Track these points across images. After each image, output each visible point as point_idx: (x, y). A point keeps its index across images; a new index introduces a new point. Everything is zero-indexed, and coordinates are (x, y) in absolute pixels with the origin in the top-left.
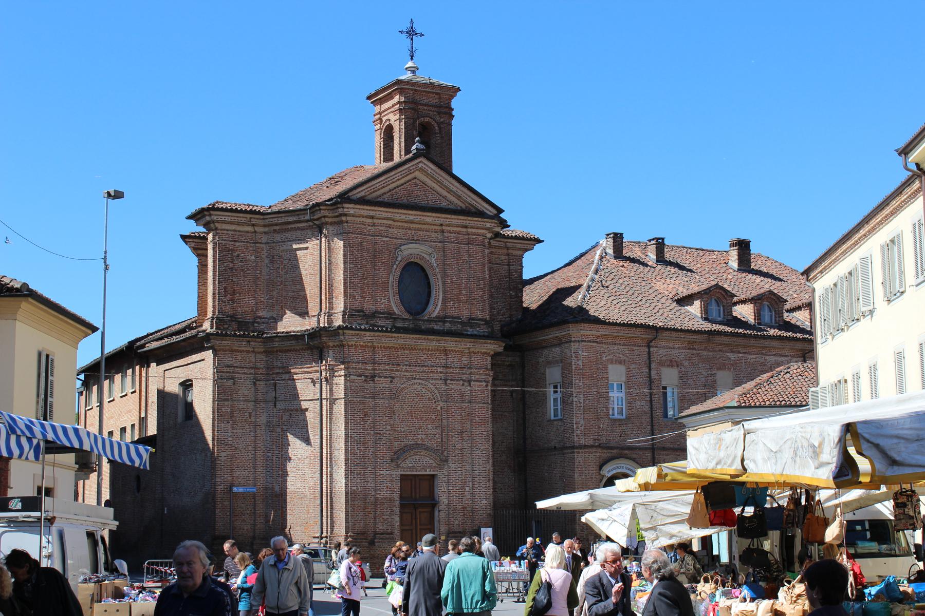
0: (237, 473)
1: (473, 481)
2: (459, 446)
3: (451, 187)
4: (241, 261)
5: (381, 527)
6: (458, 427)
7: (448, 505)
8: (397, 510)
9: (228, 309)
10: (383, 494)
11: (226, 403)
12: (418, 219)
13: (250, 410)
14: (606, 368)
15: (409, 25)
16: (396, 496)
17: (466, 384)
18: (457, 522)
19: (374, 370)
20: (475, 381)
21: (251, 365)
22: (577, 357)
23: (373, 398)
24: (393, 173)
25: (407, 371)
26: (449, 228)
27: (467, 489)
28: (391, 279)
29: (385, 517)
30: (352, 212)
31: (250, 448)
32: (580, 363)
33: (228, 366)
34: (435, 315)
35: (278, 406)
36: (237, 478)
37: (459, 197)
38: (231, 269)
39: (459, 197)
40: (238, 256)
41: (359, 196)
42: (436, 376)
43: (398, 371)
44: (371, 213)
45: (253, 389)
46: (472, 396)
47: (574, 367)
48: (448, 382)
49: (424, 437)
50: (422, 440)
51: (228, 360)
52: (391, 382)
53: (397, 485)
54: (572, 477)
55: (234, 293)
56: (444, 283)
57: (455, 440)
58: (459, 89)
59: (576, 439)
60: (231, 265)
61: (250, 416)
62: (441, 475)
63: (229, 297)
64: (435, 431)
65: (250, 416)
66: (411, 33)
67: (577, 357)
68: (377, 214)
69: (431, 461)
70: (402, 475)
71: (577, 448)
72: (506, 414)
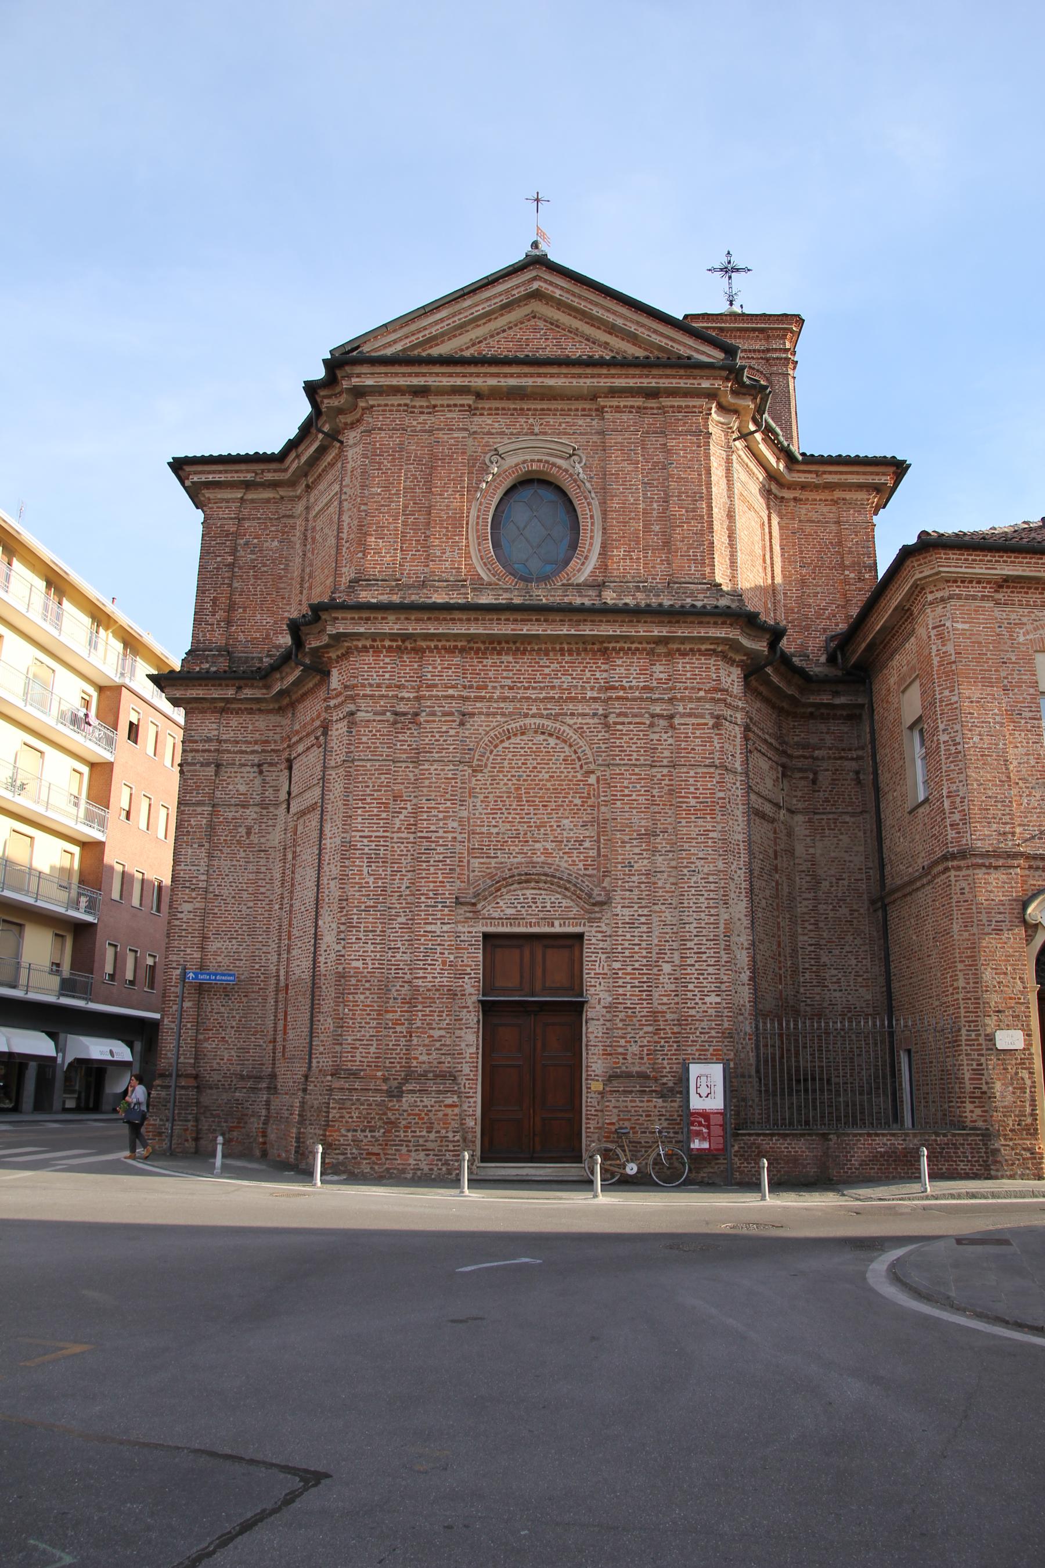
0: (214, 946)
1: (683, 948)
2: (642, 865)
3: (611, 318)
4: (252, 552)
5: (422, 1058)
6: (641, 821)
7: (610, 1008)
8: (472, 1017)
9: (218, 638)
10: (433, 976)
11: (199, 809)
12: (528, 382)
13: (249, 822)
14: (1030, 661)
15: (725, 260)
16: (471, 989)
17: (663, 723)
18: (634, 1048)
19: (418, 699)
20: (683, 715)
21: (257, 736)
22: (940, 636)
23: (417, 762)
24: (468, 302)
25: (504, 699)
26: (614, 402)
27: (667, 968)
28: (474, 513)
29: (437, 1034)
30: (369, 382)
31: (245, 895)
32: (950, 648)
33: (209, 740)
34: (581, 580)
35: (293, 810)
36: (215, 954)
37: (633, 339)
38: (232, 565)
39: (633, 339)
40: (247, 544)
41: (389, 352)
42: (581, 708)
43: (482, 699)
44: (416, 381)
45: (258, 782)
46: (679, 749)
47: (936, 661)
48: (612, 719)
49: (550, 846)
50: (546, 852)
51: (209, 726)
52: (462, 724)
53: (474, 958)
54: (947, 932)
55: (231, 608)
56: (604, 513)
57: (632, 851)
58: (799, 320)
59: (951, 834)
60: (230, 559)
61: (248, 834)
62: (591, 933)
63: (220, 614)
64: (582, 833)
65: (248, 833)
66: (729, 270)
67: (940, 636)
68: (431, 381)
69: (565, 903)
70: (486, 936)
71: (953, 857)
72: (847, 819)
